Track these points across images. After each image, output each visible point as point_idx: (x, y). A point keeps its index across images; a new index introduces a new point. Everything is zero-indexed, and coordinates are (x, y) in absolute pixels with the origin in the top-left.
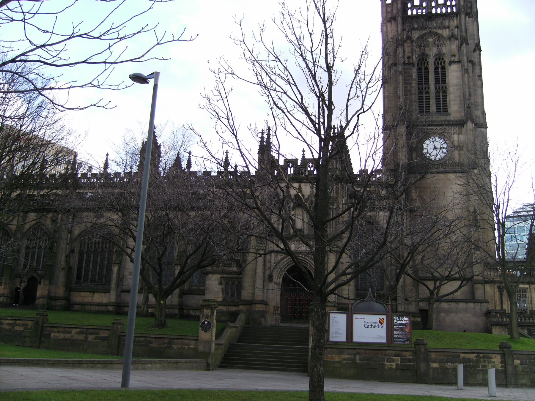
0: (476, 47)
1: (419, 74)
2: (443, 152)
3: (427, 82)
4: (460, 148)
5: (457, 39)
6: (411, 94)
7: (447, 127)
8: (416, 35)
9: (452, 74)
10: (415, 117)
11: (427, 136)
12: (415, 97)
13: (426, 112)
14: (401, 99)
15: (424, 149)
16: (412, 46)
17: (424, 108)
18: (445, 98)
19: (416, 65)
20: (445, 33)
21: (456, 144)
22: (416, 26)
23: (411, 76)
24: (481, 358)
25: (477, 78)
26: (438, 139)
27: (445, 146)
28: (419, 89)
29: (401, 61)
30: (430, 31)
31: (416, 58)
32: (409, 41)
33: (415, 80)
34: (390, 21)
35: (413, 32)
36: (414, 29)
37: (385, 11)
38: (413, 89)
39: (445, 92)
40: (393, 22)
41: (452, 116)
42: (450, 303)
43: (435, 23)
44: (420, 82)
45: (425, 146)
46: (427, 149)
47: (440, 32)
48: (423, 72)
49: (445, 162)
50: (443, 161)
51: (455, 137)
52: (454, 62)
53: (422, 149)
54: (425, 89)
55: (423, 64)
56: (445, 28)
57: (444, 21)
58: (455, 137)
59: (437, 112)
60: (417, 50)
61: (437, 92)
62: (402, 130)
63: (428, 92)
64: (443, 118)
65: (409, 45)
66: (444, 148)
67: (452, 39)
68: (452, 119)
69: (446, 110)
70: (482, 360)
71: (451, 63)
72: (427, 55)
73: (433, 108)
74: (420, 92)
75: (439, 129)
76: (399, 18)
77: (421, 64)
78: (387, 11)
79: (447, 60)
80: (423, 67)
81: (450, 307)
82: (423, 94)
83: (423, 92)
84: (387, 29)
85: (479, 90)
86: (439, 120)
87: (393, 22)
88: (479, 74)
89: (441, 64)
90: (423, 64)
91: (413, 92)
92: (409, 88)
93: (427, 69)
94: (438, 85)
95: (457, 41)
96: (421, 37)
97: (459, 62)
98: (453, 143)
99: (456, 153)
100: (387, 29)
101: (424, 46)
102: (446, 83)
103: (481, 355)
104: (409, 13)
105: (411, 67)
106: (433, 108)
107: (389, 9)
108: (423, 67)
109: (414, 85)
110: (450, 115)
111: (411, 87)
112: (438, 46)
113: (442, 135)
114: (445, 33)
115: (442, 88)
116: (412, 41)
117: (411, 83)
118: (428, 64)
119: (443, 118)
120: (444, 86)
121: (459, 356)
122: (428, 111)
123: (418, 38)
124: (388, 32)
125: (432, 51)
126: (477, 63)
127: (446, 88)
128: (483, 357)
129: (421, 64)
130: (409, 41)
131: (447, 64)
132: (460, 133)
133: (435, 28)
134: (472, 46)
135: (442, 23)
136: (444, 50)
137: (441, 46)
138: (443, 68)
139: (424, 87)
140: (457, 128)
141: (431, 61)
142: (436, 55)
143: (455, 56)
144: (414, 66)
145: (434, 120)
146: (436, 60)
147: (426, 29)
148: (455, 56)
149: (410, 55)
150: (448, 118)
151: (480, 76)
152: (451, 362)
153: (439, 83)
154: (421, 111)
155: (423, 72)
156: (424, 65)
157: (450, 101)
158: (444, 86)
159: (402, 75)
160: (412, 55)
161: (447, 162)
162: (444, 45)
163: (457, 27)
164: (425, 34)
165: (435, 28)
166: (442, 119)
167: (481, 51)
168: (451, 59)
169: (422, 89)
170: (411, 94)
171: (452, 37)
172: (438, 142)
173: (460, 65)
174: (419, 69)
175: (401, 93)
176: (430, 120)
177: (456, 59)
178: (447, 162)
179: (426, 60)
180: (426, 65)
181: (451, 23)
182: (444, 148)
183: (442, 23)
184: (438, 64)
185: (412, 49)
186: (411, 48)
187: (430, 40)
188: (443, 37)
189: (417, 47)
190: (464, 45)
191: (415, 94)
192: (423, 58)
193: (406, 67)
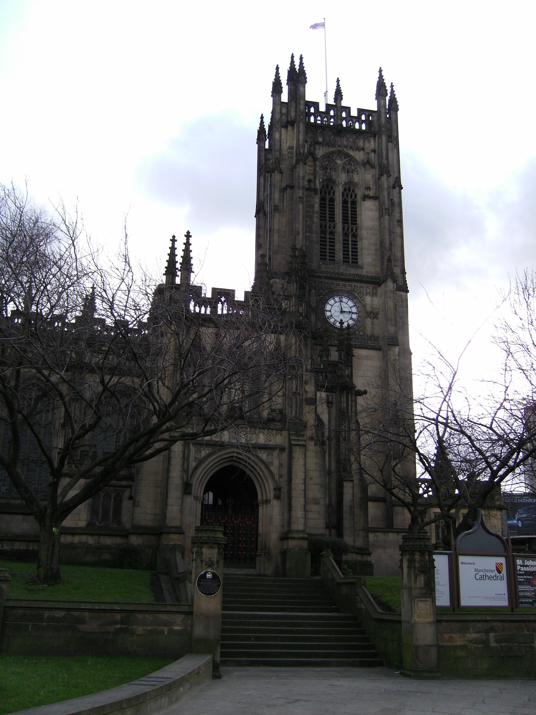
0: (395, 182)
1: (322, 206)
2: (351, 318)
4: (373, 315)
5: (373, 167)
7: (358, 284)
8: (320, 152)
9: (366, 212)
10: (315, 264)
11: (332, 294)
12: (316, 237)
13: (330, 260)
14: (301, 237)
15: (327, 311)
16: (315, 165)
18: (355, 244)
21: (369, 309)
22: (320, 140)
25: (396, 223)
26: (345, 300)
27: (354, 310)
28: (321, 226)
30: (339, 151)
31: (320, 183)
32: (310, 158)
33: (317, 214)
34: (286, 127)
35: (317, 146)
36: (318, 143)
38: (314, 225)
39: (355, 236)
40: (289, 128)
41: (364, 270)
42: (376, 534)
43: (346, 141)
44: (322, 218)
45: (328, 307)
46: (330, 311)
47: (351, 153)
51: (368, 299)
53: (324, 310)
54: (330, 228)
55: (327, 193)
56: (358, 149)
57: (357, 141)
58: (368, 299)
59: (344, 261)
61: (345, 235)
63: (332, 233)
64: (353, 271)
66: (353, 313)
67: (367, 166)
68: (364, 273)
69: (355, 261)
71: (366, 197)
72: (334, 182)
73: (339, 255)
74: (323, 232)
75: (348, 286)
76: (301, 124)
77: (325, 193)
78: (281, 112)
79: (360, 193)
80: (328, 197)
81: (376, 538)
82: (326, 235)
84: (281, 136)
85: (399, 240)
86: (348, 273)
87: (289, 128)
88: (399, 219)
89: (351, 197)
90: (327, 193)
91: (314, 228)
93: (332, 200)
94: (346, 226)
95: (374, 170)
96: (327, 156)
97: (375, 198)
98: (364, 306)
99: (369, 321)
100: (281, 136)
101: (330, 169)
104: (312, 120)
106: (339, 255)
107: (284, 110)
108: (328, 197)
110: (361, 267)
112: (348, 172)
113: (351, 296)
114: (359, 156)
115: (352, 230)
116: (315, 159)
118: (334, 194)
119: (353, 271)
120: (355, 228)
123: (323, 156)
124: (282, 141)
125: (342, 178)
126: (396, 204)
127: (356, 231)
129: (325, 193)
131: (359, 198)
132: (374, 294)
133: (346, 147)
134: (392, 180)
136: (356, 178)
137: (352, 172)
138: (354, 203)
139: (328, 225)
140: (371, 286)
141: (339, 191)
142: (346, 184)
144: (316, 194)
145: (341, 271)
146: (345, 190)
147: (333, 146)
148: (370, 188)
149: (312, 177)
150: (359, 272)
151: (400, 221)
153: (348, 223)
154: (323, 258)
156: (329, 194)
157: (362, 249)
158: (355, 228)
159: (303, 202)
160: (315, 178)
161: (357, 332)
162: (356, 173)
163: (374, 151)
164: (332, 153)
165: (346, 147)
166: (352, 272)
167: (402, 188)
168: (365, 193)
169: (326, 227)
171: (368, 163)
172: (348, 304)
173: (376, 203)
174: (322, 199)
175: (301, 227)
176: (336, 271)
177: (371, 193)
178: (357, 332)
179: (332, 189)
180: (331, 195)
181: (367, 145)
182: (353, 313)
184: (347, 196)
185: (315, 170)
186: (312, 168)
188: (356, 161)
189: (321, 168)
190: (385, 175)
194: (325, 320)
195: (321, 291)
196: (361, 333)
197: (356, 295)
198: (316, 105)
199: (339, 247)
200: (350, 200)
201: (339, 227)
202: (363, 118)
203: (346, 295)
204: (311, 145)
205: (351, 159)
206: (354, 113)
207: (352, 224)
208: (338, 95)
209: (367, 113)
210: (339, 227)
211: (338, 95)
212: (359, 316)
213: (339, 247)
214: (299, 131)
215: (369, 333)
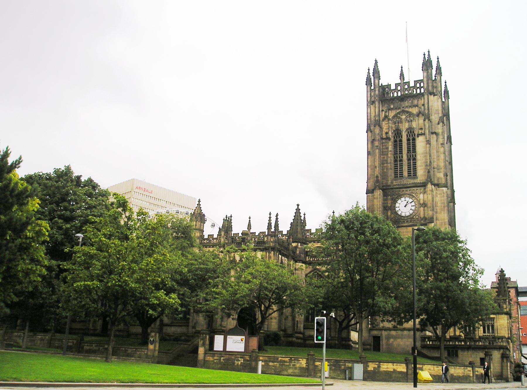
1: (395, 146)
3: (401, 152)
4: (424, 205)
6: (387, 163)
7: (415, 189)
8: (392, 114)
11: (400, 196)
12: (390, 165)
14: (377, 168)
17: (398, 174)
18: (415, 164)
19: (392, 139)
20: (415, 111)
21: (422, 202)
23: (387, 148)
24: (293, 360)
28: (395, 158)
29: (378, 137)
30: (403, 110)
31: (392, 133)
35: (390, 111)
36: (390, 109)
37: (369, 95)
38: (389, 159)
39: (415, 159)
44: (395, 153)
45: (397, 205)
47: (410, 110)
48: (398, 143)
49: (413, 218)
50: (412, 216)
52: (422, 134)
53: (395, 207)
58: (421, 196)
59: (408, 176)
60: (393, 126)
61: (409, 160)
62: (378, 193)
64: (411, 181)
65: (387, 123)
69: (415, 175)
70: (293, 361)
71: (418, 135)
72: (400, 130)
73: (405, 174)
74: (396, 161)
75: (408, 191)
79: (416, 133)
80: (398, 140)
81: (397, 334)
83: (398, 161)
84: (371, 110)
91: (389, 161)
92: (386, 158)
93: (401, 141)
96: (395, 116)
97: (424, 134)
98: (419, 201)
99: (422, 209)
100: (371, 110)
101: (398, 123)
102: (415, 152)
103: (293, 359)
105: (388, 141)
106: (405, 174)
108: (398, 140)
109: (389, 155)
111: (387, 157)
112: (409, 122)
113: (411, 196)
114: (415, 111)
115: (413, 156)
116: (389, 119)
117: (387, 154)
118: (402, 137)
119: (411, 181)
121: (278, 359)
122: (402, 176)
123: (394, 117)
125: (404, 127)
126: (440, 133)
127: (415, 156)
128: (294, 360)
130: (387, 120)
132: (425, 193)
133: (407, 107)
135: (412, 102)
136: (414, 125)
137: (411, 121)
138: (414, 139)
142: (407, 129)
143: (422, 129)
147: (399, 108)
149: (387, 131)
150: (415, 181)
152: (272, 362)
155: (398, 143)
156: (399, 137)
159: (378, 149)
164: (399, 113)
165: (407, 107)
166: (411, 182)
169: (397, 158)
170: (387, 163)
176: (402, 183)
179: (400, 134)
183: (412, 102)
184: (410, 136)
187: (404, 117)
188: (413, 114)
190: (427, 120)
191: (391, 163)
192: (398, 133)
193: (384, 141)
194: (396, 213)
195: (393, 196)
196: (417, 217)
197: (414, 195)
198: (389, 86)
200: (411, 138)
201: (405, 157)
202: (418, 85)
203: (408, 196)
204: (386, 112)
205: (410, 114)
207: (413, 152)
208: (402, 75)
209: (420, 82)
210: (405, 157)
211: (402, 75)
212: (416, 207)
214: (375, 107)
215: (422, 216)
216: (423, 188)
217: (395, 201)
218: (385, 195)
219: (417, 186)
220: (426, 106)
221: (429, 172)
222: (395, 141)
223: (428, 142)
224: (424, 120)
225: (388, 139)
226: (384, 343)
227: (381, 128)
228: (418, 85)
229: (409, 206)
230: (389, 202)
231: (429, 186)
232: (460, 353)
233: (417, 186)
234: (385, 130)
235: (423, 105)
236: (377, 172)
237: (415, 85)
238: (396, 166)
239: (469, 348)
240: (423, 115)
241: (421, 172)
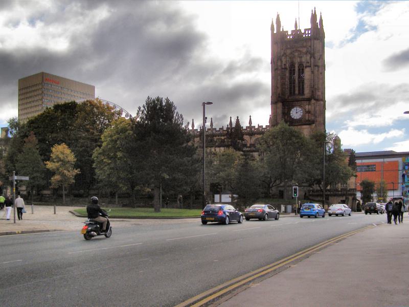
4: (309, 112)
6: (285, 85)
11: (293, 107)
18: (303, 86)
21: (307, 110)
23: (286, 75)
29: (280, 68)
38: (286, 82)
47: (301, 50)
48: (292, 72)
49: (301, 120)
52: (308, 66)
53: (290, 114)
58: (307, 107)
62: (280, 105)
63: (294, 83)
64: (301, 97)
71: (306, 67)
73: (297, 92)
79: (305, 65)
93: (294, 70)
98: (305, 110)
99: (307, 114)
106: (297, 92)
113: (300, 106)
116: (286, 56)
122: (294, 94)
125: (297, 60)
132: (309, 105)
136: (303, 60)
138: (303, 70)
141: (297, 66)
143: (308, 63)
148: (308, 63)
149: (285, 63)
150: (304, 97)
155: (292, 72)
172: (299, 109)
177: (309, 64)
187: (296, 54)
199: (297, 89)
206: (303, 32)
213: (297, 89)
216: (308, 102)
217: (289, 110)
218: (283, 105)
219: (304, 100)
220: (312, 48)
221: (313, 92)
222: (290, 70)
223: (313, 72)
224: (311, 58)
225: (286, 68)
226: (285, 194)
227: (282, 62)
228: (307, 32)
229: (299, 113)
230: (286, 110)
231: (313, 101)
232: (330, 198)
233: (304, 100)
234: (284, 63)
235: (310, 47)
236: (279, 90)
237: (305, 32)
238: (291, 88)
239: (335, 195)
240: (309, 53)
241: (307, 92)
